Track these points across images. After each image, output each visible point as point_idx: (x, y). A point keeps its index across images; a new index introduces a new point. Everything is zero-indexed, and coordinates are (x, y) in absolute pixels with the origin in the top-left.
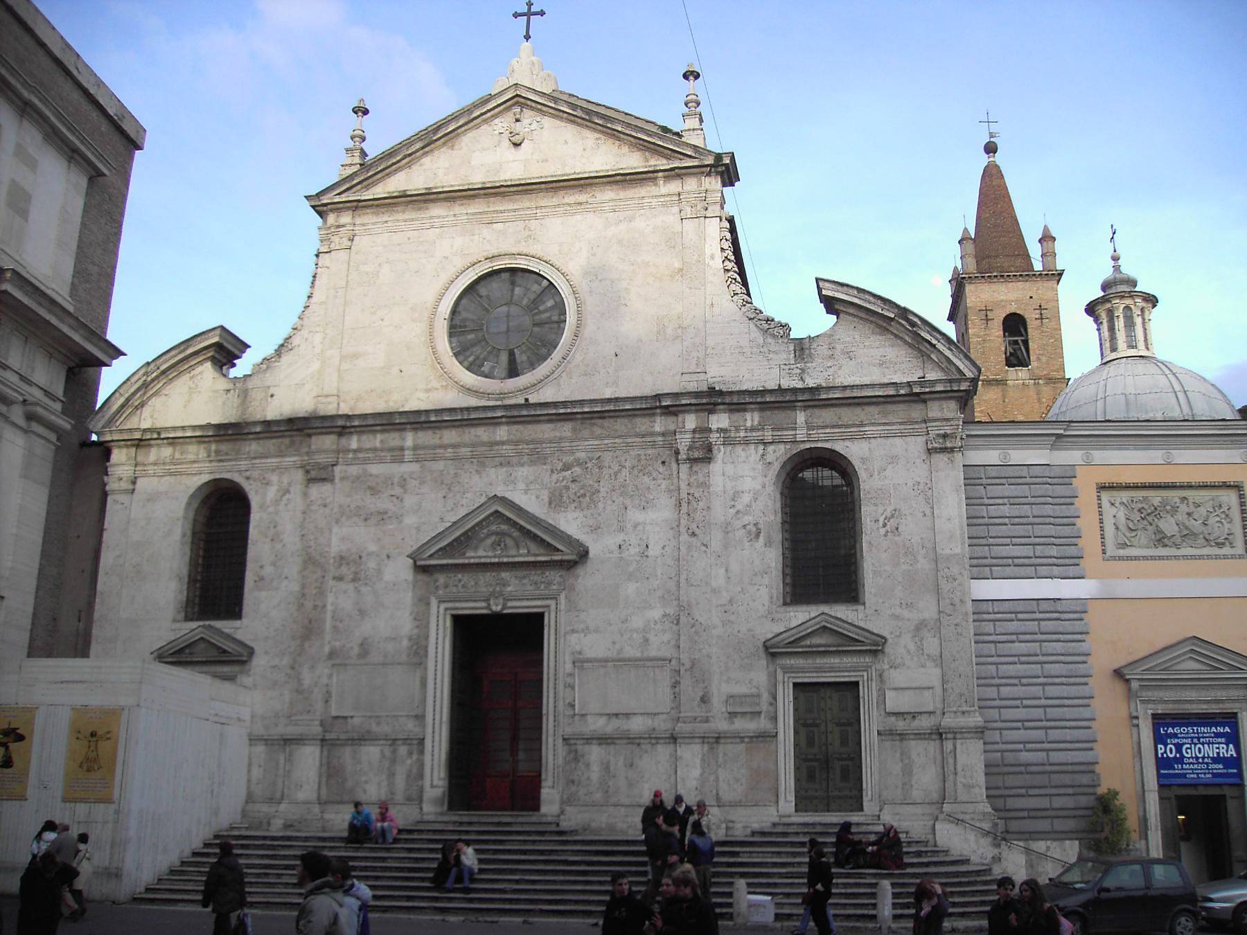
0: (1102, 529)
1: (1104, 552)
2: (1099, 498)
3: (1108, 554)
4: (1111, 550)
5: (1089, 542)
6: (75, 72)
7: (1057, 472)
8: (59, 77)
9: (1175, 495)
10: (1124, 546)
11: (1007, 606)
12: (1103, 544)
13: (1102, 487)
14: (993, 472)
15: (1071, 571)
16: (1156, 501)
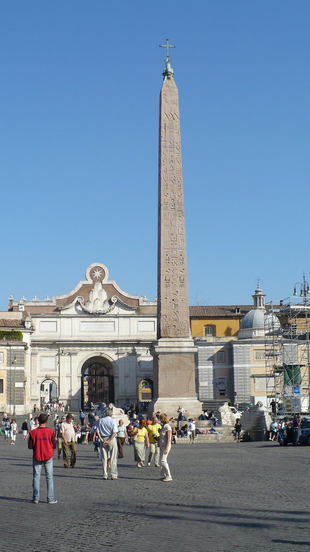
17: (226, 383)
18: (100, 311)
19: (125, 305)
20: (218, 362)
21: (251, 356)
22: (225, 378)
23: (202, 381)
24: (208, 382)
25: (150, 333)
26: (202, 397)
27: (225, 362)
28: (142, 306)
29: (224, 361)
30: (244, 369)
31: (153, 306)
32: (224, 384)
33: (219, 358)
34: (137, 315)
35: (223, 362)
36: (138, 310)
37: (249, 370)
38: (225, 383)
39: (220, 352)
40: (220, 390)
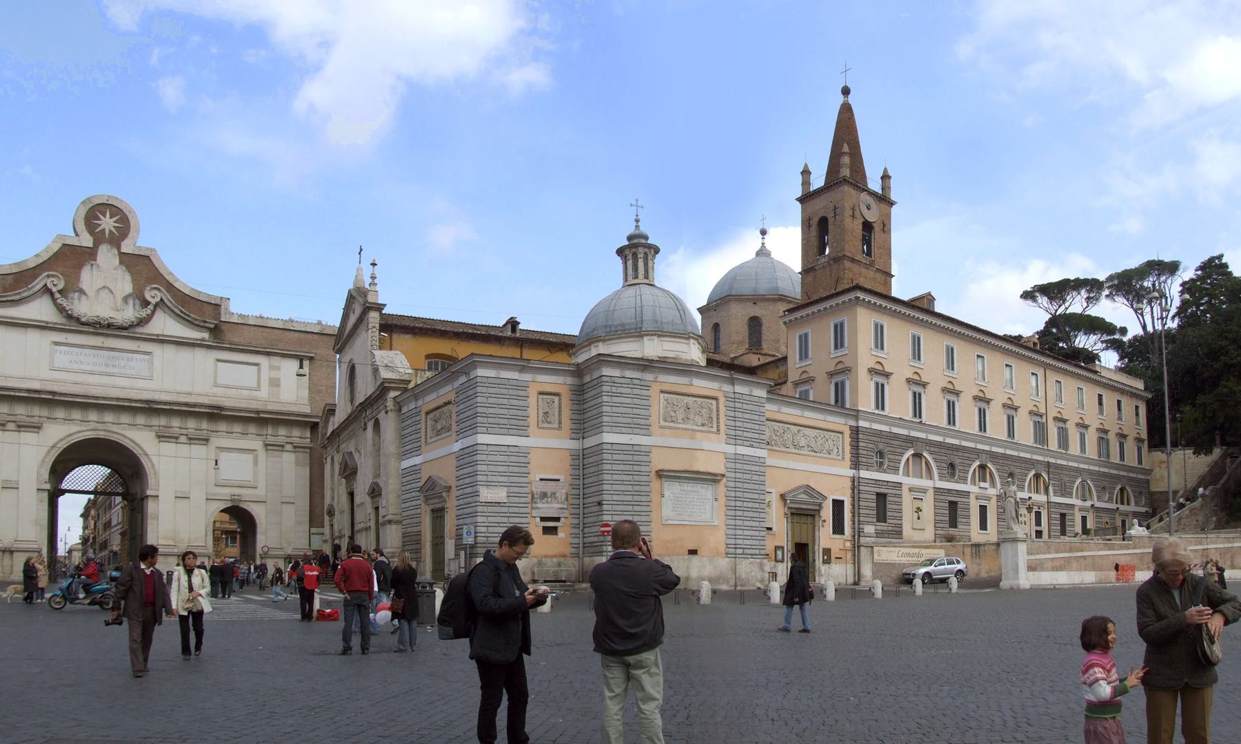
0: (426, 432)
1: (426, 442)
2: (426, 418)
3: (428, 442)
4: (429, 441)
5: (423, 440)
6: (292, 328)
7: (418, 410)
8: (288, 333)
9: (440, 411)
10: (431, 438)
11: (410, 470)
12: (426, 438)
13: (427, 413)
14: (407, 415)
15: (418, 453)
16: (438, 415)
17: (564, 497)
18: (110, 318)
19: (182, 312)
20: (540, 428)
21: (654, 411)
22: (559, 480)
23: (488, 484)
24: (506, 489)
25: (246, 393)
26: (486, 538)
27: (560, 428)
28: (227, 324)
29: (556, 425)
30: (634, 449)
31: (255, 326)
32: (555, 498)
33: (541, 414)
34: (215, 344)
35: (554, 429)
36: (216, 331)
37: (648, 453)
38: (557, 495)
39: (544, 397)
40: (543, 519)
